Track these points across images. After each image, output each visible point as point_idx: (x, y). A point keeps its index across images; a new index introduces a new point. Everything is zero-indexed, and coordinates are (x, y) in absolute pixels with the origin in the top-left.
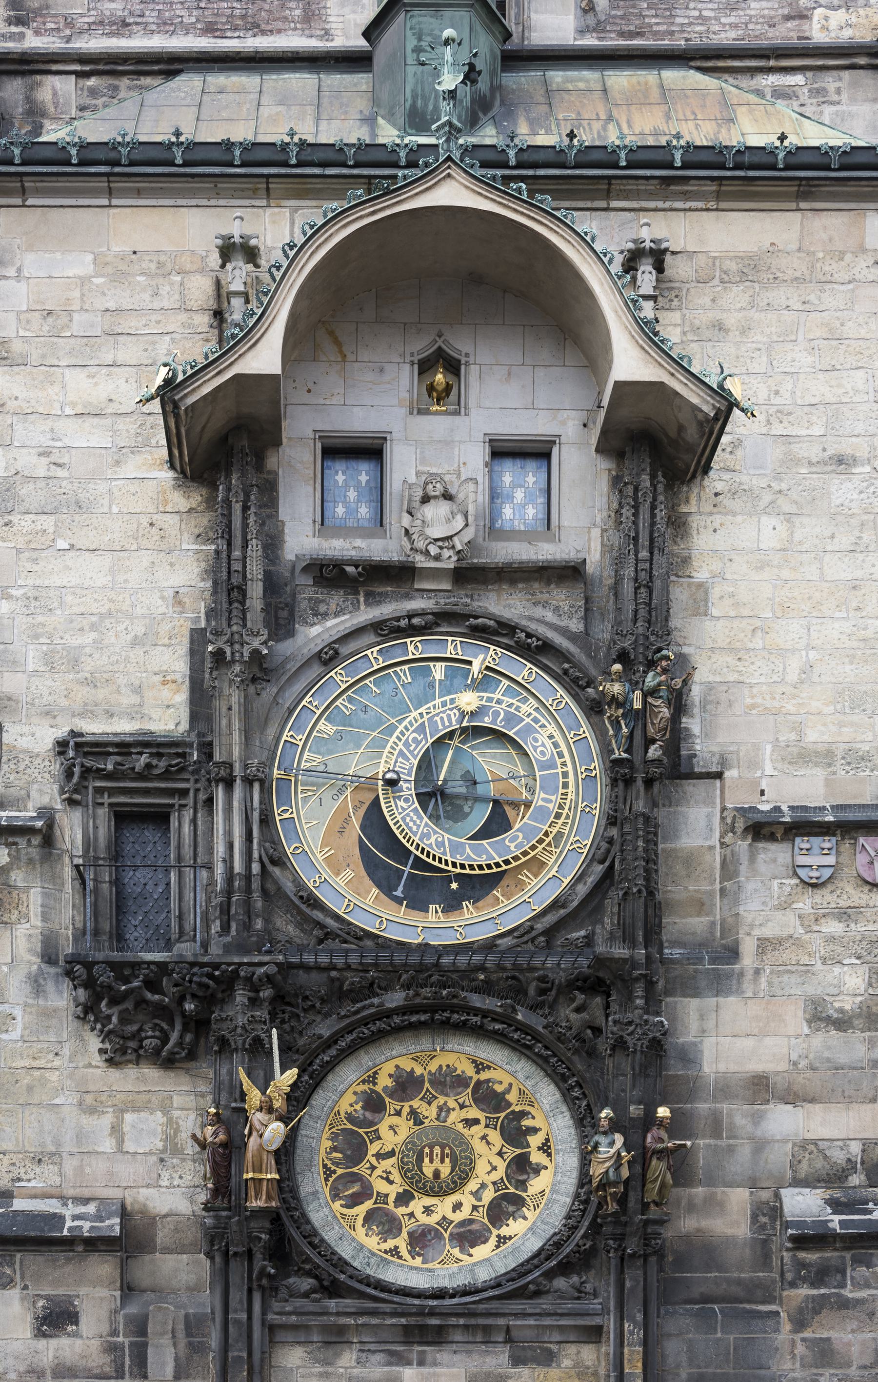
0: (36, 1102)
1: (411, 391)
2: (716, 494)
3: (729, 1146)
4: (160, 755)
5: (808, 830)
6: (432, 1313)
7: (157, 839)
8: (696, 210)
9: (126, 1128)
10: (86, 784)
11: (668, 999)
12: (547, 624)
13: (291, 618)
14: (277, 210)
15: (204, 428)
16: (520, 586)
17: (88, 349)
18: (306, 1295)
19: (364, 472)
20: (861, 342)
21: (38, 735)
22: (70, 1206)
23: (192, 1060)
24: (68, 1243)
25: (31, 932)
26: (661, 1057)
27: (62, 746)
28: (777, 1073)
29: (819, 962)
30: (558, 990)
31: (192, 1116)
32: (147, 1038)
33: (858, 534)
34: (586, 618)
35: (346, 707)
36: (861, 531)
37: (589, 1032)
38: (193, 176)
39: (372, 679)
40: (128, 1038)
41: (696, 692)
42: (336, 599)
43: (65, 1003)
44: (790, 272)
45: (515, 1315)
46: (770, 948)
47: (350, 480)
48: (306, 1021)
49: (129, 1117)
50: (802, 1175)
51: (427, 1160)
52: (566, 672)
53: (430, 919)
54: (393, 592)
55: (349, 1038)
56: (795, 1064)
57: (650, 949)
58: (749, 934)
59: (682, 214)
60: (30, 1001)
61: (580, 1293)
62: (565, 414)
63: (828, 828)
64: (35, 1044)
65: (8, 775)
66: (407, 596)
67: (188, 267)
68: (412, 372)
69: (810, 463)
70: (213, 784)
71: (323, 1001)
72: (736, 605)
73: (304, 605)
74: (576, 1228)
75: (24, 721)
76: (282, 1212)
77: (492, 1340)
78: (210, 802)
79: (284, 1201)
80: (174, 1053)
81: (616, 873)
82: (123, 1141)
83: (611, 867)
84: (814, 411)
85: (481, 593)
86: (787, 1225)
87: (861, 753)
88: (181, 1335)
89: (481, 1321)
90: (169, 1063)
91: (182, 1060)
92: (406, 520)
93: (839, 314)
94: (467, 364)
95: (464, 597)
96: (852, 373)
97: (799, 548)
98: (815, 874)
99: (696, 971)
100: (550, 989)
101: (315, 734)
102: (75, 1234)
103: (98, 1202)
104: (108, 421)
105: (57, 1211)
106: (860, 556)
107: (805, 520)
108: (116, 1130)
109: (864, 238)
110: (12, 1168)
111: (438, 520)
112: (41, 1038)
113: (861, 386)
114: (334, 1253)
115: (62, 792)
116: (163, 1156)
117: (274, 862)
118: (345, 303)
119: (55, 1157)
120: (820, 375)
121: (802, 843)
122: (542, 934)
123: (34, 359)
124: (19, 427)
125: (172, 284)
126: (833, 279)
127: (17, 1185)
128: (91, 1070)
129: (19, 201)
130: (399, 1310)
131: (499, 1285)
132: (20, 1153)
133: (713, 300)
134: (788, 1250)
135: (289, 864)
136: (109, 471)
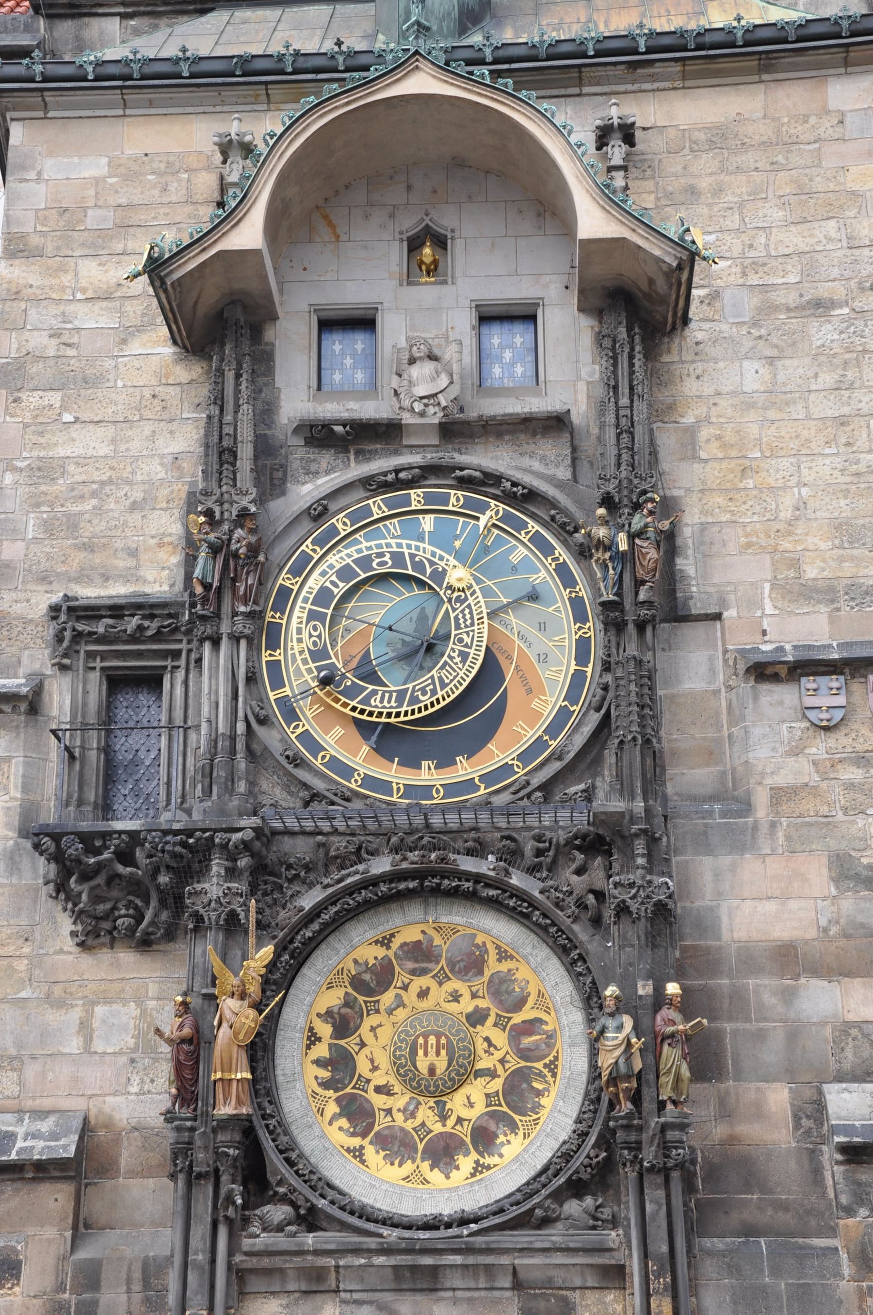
1: (400, 265)
2: (697, 343)
4: (152, 617)
5: (814, 669)
6: (425, 1251)
8: (664, 90)
10: (77, 648)
11: (678, 858)
13: (284, 480)
16: (507, 438)
20: (830, 195)
21: (33, 601)
25: (9, 804)
26: (671, 924)
27: (55, 610)
29: (840, 813)
32: (120, 917)
33: (842, 373)
36: (845, 369)
39: (362, 533)
40: (101, 918)
41: (687, 534)
42: (326, 458)
44: (757, 137)
45: (521, 1250)
48: (290, 893)
50: (847, 1066)
51: (421, 1052)
52: (553, 519)
53: (423, 777)
54: (382, 449)
55: (333, 910)
57: (651, 802)
61: (596, 1221)
66: (396, 453)
67: (195, 165)
68: (401, 248)
69: (789, 309)
73: (295, 465)
74: (587, 1134)
75: (20, 587)
77: (497, 1285)
78: (199, 661)
79: (260, 1107)
80: (148, 934)
83: (608, 715)
84: (789, 261)
85: (469, 446)
86: (835, 1130)
87: (864, 588)
88: (137, 1287)
90: (145, 944)
91: (158, 941)
92: (395, 382)
93: (807, 171)
94: (452, 238)
95: (452, 453)
96: (823, 223)
97: (783, 389)
98: (825, 716)
99: (706, 825)
100: (548, 850)
106: (847, 394)
107: (787, 362)
109: (826, 101)
113: (833, 235)
117: (263, 721)
120: (792, 228)
121: (809, 683)
122: (539, 788)
123: (49, 250)
124: (32, 313)
125: (179, 181)
126: (799, 140)
129: (41, 114)
131: (501, 1211)
134: (838, 1163)
135: (276, 723)
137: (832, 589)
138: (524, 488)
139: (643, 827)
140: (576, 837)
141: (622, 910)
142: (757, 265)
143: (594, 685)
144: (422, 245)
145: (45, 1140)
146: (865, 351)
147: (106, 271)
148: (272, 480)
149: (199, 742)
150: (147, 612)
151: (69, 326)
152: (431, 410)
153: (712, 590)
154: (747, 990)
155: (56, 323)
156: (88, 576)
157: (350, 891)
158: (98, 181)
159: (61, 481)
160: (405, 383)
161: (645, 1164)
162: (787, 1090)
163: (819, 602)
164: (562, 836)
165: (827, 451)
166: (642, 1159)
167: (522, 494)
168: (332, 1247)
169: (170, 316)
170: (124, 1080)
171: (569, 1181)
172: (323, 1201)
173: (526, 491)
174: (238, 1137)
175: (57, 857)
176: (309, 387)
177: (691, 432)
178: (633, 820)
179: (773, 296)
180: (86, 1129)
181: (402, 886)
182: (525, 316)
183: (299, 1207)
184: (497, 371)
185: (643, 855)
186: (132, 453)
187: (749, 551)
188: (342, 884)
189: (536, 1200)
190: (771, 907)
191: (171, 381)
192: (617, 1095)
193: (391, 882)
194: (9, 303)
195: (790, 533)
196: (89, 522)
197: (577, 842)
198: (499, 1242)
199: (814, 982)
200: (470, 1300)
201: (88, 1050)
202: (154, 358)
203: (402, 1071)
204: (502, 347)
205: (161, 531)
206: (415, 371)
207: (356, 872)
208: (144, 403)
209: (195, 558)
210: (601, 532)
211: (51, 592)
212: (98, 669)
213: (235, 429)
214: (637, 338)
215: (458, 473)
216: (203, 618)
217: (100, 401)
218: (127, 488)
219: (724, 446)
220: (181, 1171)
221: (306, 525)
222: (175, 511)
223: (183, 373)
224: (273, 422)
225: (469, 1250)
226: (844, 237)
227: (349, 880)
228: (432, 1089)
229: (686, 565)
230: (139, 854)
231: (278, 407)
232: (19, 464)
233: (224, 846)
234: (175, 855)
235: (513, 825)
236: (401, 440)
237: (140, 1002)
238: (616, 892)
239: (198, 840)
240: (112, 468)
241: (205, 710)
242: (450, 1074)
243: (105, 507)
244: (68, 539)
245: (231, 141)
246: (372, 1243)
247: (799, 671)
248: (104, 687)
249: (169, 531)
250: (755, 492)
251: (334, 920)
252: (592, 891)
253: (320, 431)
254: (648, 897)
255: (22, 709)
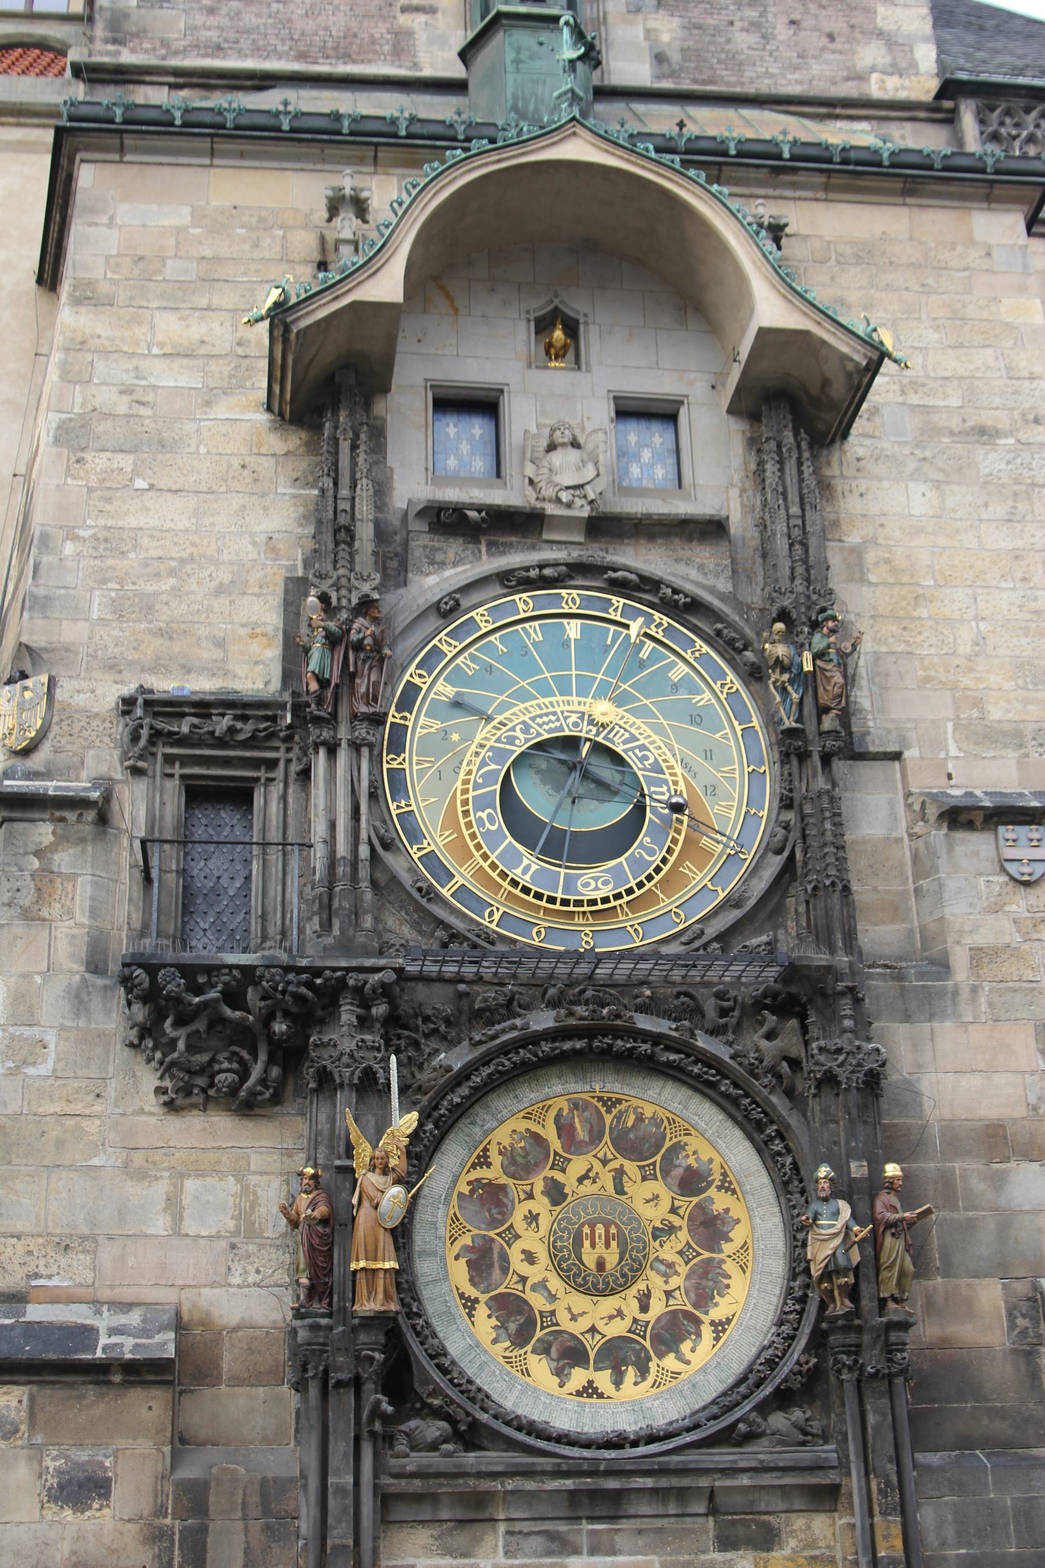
0: (67, 1163)
2: (858, 459)
3: (969, 1220)
4: (245, 718)
6: (609, 1473)
7: (235, 821)
8: (805, 199)
9: (186, 1201)
10: (154, 750)
12: (693, 582)
14: (384, 177)
15: (311, 361)
16: (660, 541)
17: (181, 293)
18: (434, 1447)
19: (478, 427)
21: (99, 692)
22: (106, 1314)
23: (277, 1104)
24: (98, 1372)
25: (75, 931)
27: (128, 704)
28: (1015, 1120)
30: (742, 1010)
31: (276, 1183)
34: (732, 578)
35: (468, 666)
37: (785, 1064)
38: (300, 140)
39: (497, 635)
42: (454, 547)
43: (113, 1026)
46: (985, 960)
47: (466, 434)
48: (427, 1050)
49: (191, 1185)
56: (1035, 1108)
58: (958, 943)
59: (792, 203)
60: (68, 1023)
62: (692, 376)
63: (1033, 815)
64: (70, 1082)
65: (58, 738)
66: (533, 547)
69: (952, 434)
70: (311, 750)
71: (448, 1022)
72: (893, 571)
73: (417, 552)
76: (400, 1318)
78: (305, 775)
81: (799, 864)
82: (181, 1219)
85: (617, 546)
89: (675, 1482)
91: (265, 1104)
94: (586, 323)
96: (981, 350)
98: (1026, 869)
100: (733, 1009)
101: (432, 695)
102: (113, 1355)
103: (143, 1308)
104: (200, 362)
105: (88, 1322)
106: (1019, 527)
107: (955, 488)
108: (173, 1204)
110: (28, 1259)
111: (566, 468)
112: (80, 1073)
113: (992, 364)
114: (470, 1382)
115: (124, 757)
116: (234, 1240)
117: (387, 845)
118: (458, 256)
119: (88, 1243)
120: (950, 351)
121: (1006, 832)
124: (100, 366)
125: (273, 237)
127: (34, 1283)
128: (143, 1118)
130: (564, 1468)
131: (697, 1426)
132: (40, 1236)
133: (832, 279)
136: (198, 412)
137: (1018, 734)
138: (686, 596)
139: (850, 984)
140: (765, 995)
141: (829, 1080)
142: (915, 385)
143: (772, 824)
144: (553, 326)
145: (135, 1337)
146: (1033, 485)
147: (188, 326)
148: (395, 567)
149: (307, 871)
150: (239, 712)
151: (143, 383)
152: (579, 502)
153: (891, 726)
154: (953, 1174)
155: (128, 379)
156: (165, 667)
157: (505, 1050)
158: (179, 231)
159: (132, 555)
160: (545, 471)
161: (869, 1369)
162: (1000, 1287)
163: (1006, 746)
164: (747, 993)
165: (1003, 585)
166: (863, 1365)
167: (685, 604)
168: (500, 1468)
169: (278, 374)
170: (223, 1269)
171: (777, 1390)
172: (486, 1416)
173: (688, 600)
174: (382, 1339)
175: (151, 996)
176: (427, 469)
177: (857, 553)
178: (839, 977)
179: (935, 418)
180: (180, 1325)
181: (567, 1046)
182: (663, 413)
183: (458, 1422)
184: (635, 471)
185: (851, 1017)
186: (217, 529)
187: (929, 686)
188: (498, 1041)
189: (738, 1413)
190: (975, 1081)
191: (264, 451)
192: (832, 1291)
193: (554, 1040)
194: (73, 353)
195: (970, 670)
196: (167, 603)
197: (767, 1001)
198: (697, 1461)
199: (1026, 1165)
200: (659, 1531)
201: (177, 1231)
202: (244, 424)
203: (564, 1265)
204: (640, 445)
205: (254, 619)
206: (557, 458)
207: (514, 1028)
208: (231, 474)
209: (307, 650)
210: (781, 650)
211: (122, 682)
212: (177, 777)
213: (353, 507)
214: (804, 445)
215: (611, 574)
216: (318, 721)
217: (180, 468)
218: (212, 568)
219: (893, 571)
220: (313, 1378)
221: (434, 622)
222: (269, 597)
223: (277, 443)
224: (385, 504)
225: (664, 1471)
226: (1002, 367)
227: (505, 1037)
228: (601, 1286)
229: (863, 697)
230: (251, 994)
231: (391, 488)
232: (82, 533)
233: (358, 990)
234: (299, 998)
235: (688, 980)
236: (540, 533)
237: (239, 1177)
238: (822, 1058)
239: (327, 980)
240: (194, 544)
241: (319, 830)
242: (622, 1269)
243: (187, 588)
244: (140, 622)
245: (344, 196)
246: (546, 1463)
247: (995, 819)
248: (183, 799)
249: (263, 620)
250: (930, 623)
251: (486, 1084)
252: (786, 1059)
253: (450, 515)
254: (859, 1065)
255: (90, 819)
